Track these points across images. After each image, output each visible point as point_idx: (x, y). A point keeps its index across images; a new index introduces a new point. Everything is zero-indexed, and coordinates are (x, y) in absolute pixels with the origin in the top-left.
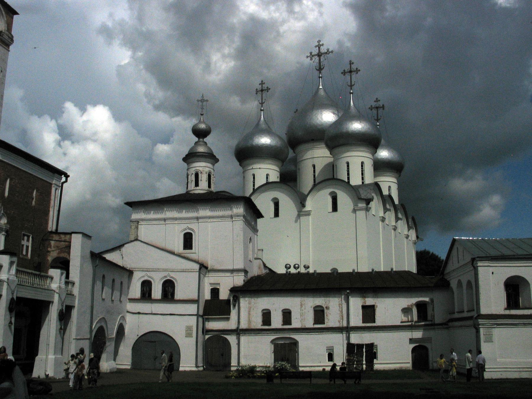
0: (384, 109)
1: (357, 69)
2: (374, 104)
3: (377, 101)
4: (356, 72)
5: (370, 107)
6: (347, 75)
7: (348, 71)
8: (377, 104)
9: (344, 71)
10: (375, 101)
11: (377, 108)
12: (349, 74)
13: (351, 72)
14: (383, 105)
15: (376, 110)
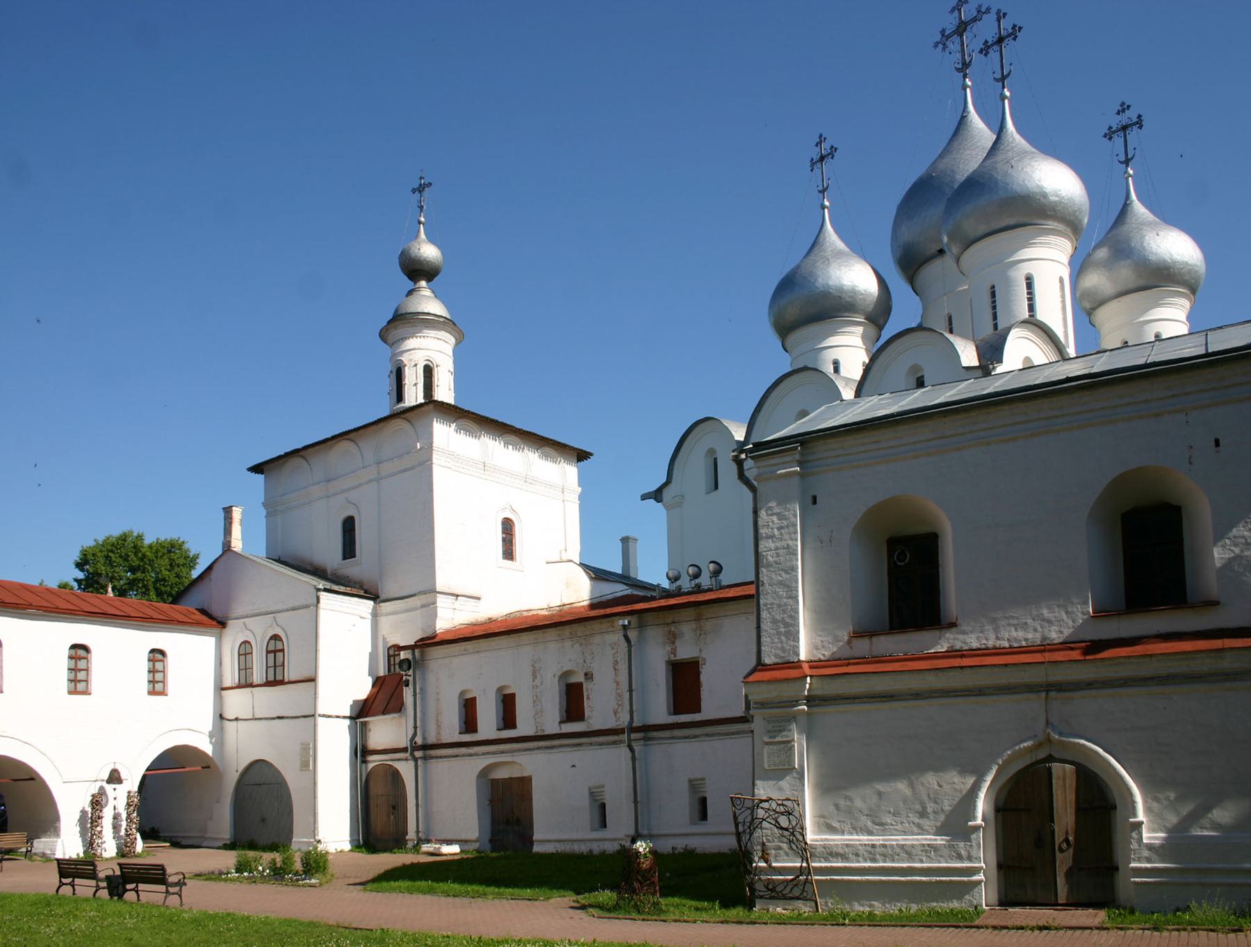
0: (1141, 127)
1: (1014, 26)
2: (1115, 122)
3: (1123, 111)
4: (1013, 36)
5: (1108, 132)
6: (993, 52)
7: (995, 40)
8: (1124, 119)
9: (986, 42)
10: (1118, 113)
11: (1124, 128)
12: (996, 48)
13: (1000, 40)
14: (1139, 116)
15: (1122, 134)
